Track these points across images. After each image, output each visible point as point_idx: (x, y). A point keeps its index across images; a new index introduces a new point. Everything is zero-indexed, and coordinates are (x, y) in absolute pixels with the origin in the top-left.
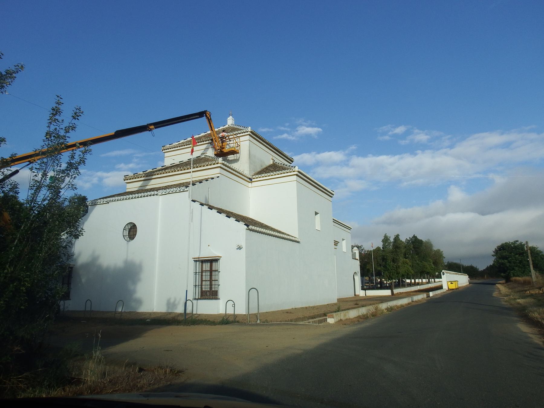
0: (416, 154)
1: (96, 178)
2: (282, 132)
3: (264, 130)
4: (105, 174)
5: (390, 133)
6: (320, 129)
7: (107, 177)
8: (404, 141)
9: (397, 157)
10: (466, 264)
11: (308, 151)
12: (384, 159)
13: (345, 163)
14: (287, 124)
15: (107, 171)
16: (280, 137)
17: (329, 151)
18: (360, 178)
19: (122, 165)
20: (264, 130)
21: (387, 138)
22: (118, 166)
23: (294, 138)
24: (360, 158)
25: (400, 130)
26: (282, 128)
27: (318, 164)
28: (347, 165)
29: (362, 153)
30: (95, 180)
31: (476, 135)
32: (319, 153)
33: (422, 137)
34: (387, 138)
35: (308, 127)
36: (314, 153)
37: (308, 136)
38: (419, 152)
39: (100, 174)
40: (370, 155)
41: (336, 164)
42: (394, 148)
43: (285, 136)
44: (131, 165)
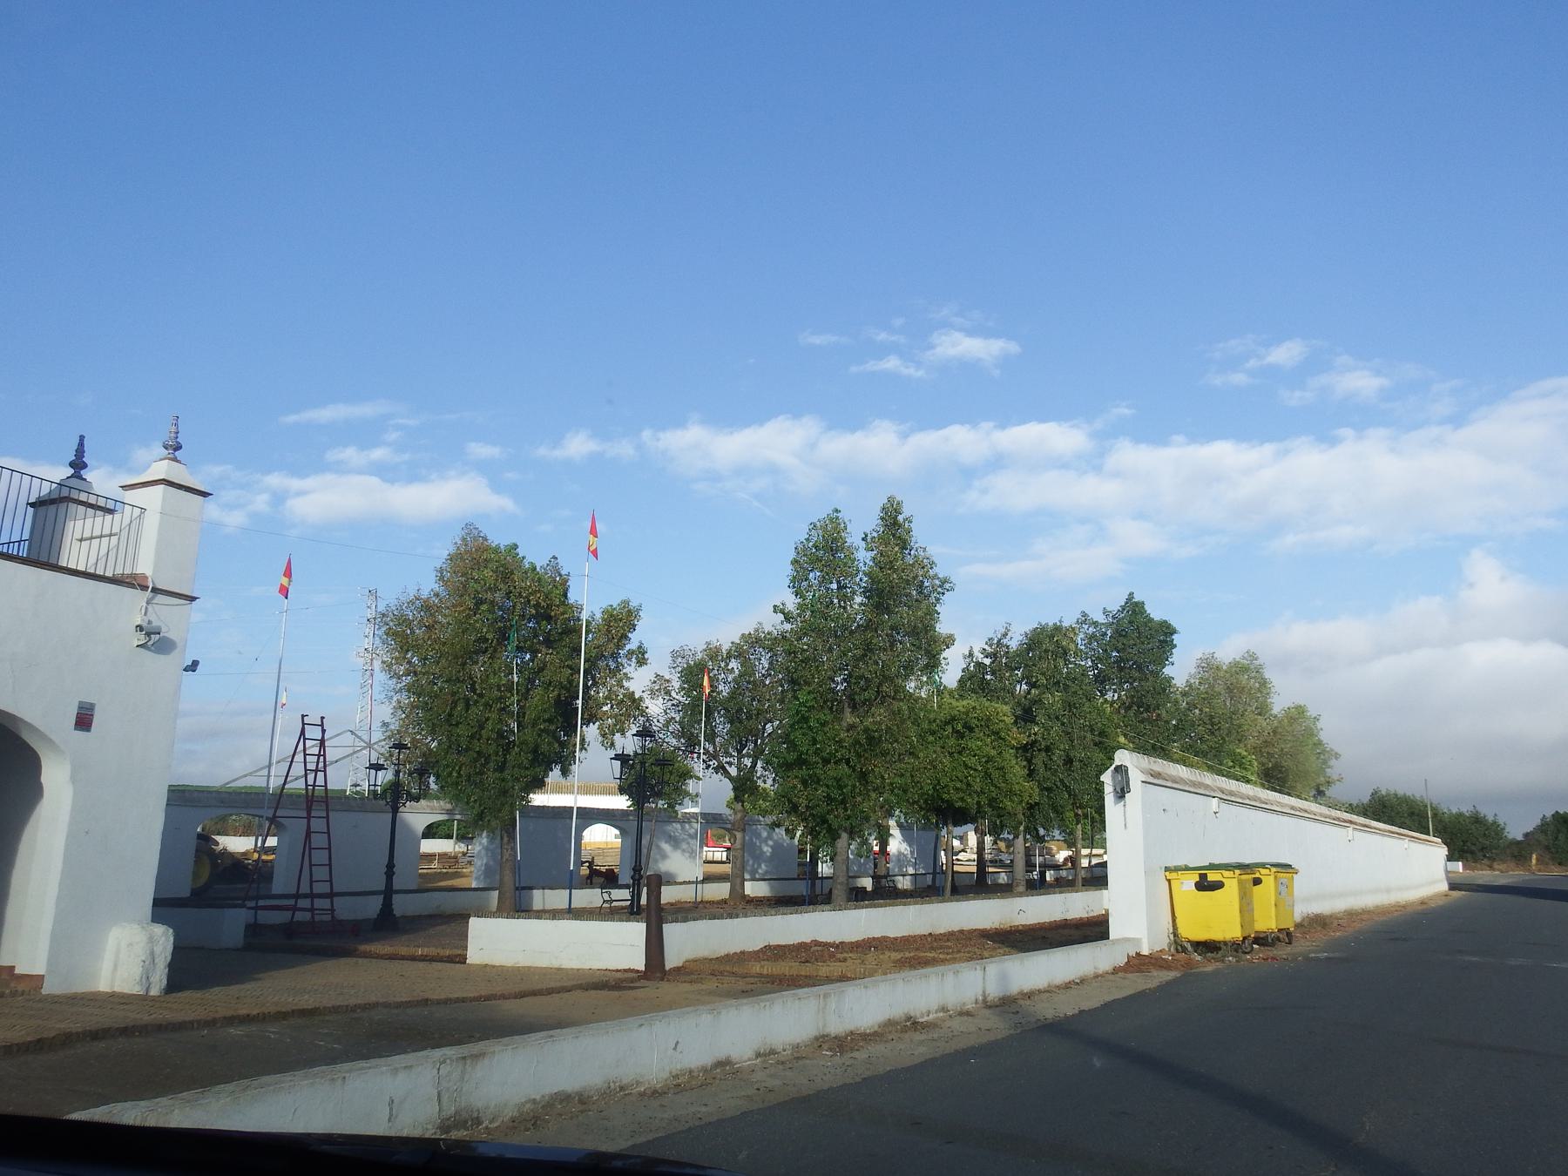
0: (1333, 442)
1: (265, 497)
2: (883, 351)
3: (817, 340)
4: (296, 484)
5: (1252, 363)
6: (1013, 348)
7: (301, 493)
8: (1298, 394)
9: (1269, 449)
10: (1456, 805)
11: (970, 419)
12: (1222, 453)
13: (1092, 462)
14: (898, 322)
15: (299, 471)
16: (873, 366)
17: (1042, 420)
18: (1140, 516)
19: (350, 454)
20: (817, 340)
21: (1239, 378)
22: (332, 456)
23: (920, 373)
24: (1143, 446)
25: (1285, 354)
26: (883, 336)
27: (998, 462)
28: (1098, 469)
29: (1152, 432)
30: (261, 502)
31: (1550, 384)
32: (1003, 426)
33: (1362, 382)
34: (1239, 378)
35: (970, 333)
36: (986, 425)
37: (968, 369)
38: (1347, 432)
39: (275, 480)
40: (1179, 438)
41: (1061, 464)
42: (1261, 417)
43: (892, 363)
44: (378, 454)
